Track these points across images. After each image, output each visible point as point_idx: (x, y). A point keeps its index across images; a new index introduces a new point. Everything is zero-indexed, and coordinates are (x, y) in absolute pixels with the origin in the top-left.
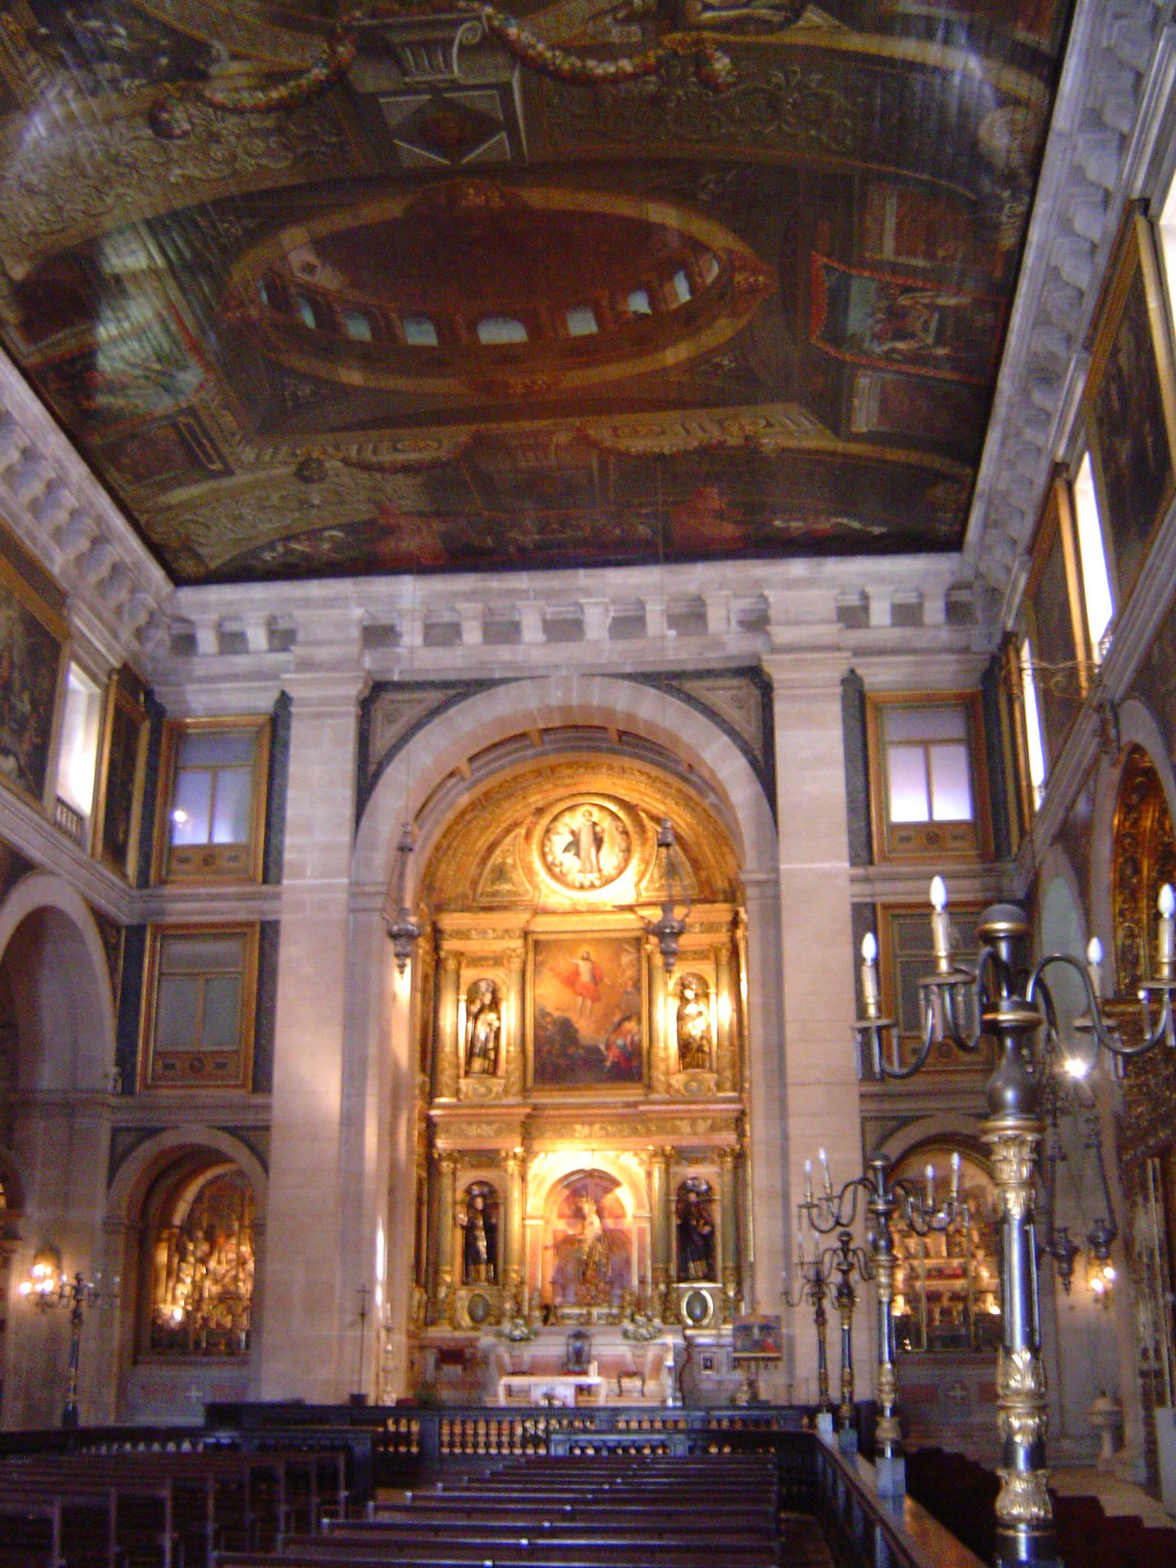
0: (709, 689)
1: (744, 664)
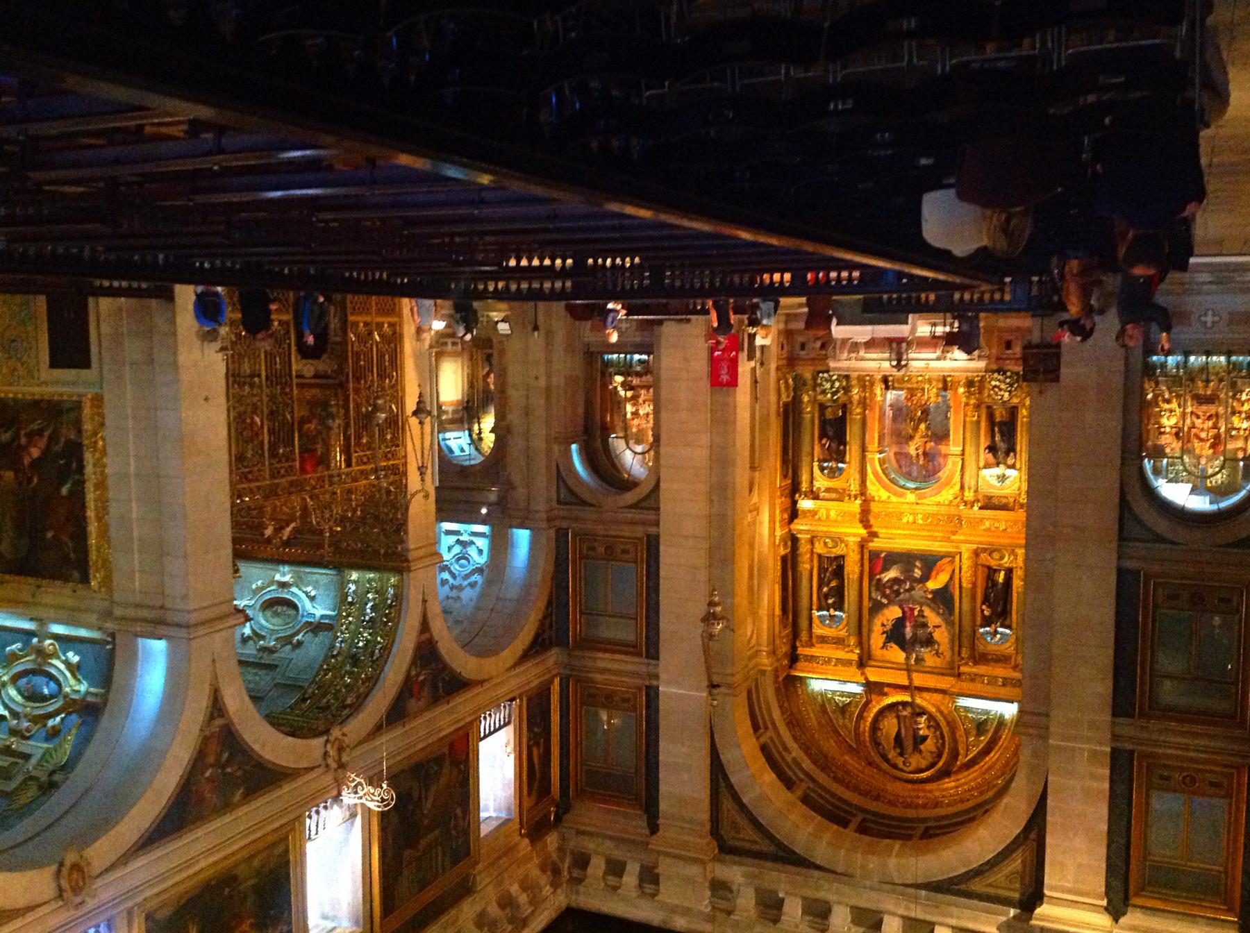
0: (755, 842)
1: (728, 857)
